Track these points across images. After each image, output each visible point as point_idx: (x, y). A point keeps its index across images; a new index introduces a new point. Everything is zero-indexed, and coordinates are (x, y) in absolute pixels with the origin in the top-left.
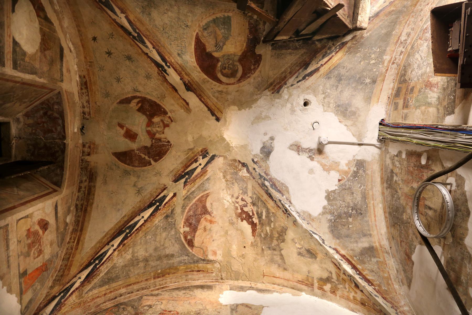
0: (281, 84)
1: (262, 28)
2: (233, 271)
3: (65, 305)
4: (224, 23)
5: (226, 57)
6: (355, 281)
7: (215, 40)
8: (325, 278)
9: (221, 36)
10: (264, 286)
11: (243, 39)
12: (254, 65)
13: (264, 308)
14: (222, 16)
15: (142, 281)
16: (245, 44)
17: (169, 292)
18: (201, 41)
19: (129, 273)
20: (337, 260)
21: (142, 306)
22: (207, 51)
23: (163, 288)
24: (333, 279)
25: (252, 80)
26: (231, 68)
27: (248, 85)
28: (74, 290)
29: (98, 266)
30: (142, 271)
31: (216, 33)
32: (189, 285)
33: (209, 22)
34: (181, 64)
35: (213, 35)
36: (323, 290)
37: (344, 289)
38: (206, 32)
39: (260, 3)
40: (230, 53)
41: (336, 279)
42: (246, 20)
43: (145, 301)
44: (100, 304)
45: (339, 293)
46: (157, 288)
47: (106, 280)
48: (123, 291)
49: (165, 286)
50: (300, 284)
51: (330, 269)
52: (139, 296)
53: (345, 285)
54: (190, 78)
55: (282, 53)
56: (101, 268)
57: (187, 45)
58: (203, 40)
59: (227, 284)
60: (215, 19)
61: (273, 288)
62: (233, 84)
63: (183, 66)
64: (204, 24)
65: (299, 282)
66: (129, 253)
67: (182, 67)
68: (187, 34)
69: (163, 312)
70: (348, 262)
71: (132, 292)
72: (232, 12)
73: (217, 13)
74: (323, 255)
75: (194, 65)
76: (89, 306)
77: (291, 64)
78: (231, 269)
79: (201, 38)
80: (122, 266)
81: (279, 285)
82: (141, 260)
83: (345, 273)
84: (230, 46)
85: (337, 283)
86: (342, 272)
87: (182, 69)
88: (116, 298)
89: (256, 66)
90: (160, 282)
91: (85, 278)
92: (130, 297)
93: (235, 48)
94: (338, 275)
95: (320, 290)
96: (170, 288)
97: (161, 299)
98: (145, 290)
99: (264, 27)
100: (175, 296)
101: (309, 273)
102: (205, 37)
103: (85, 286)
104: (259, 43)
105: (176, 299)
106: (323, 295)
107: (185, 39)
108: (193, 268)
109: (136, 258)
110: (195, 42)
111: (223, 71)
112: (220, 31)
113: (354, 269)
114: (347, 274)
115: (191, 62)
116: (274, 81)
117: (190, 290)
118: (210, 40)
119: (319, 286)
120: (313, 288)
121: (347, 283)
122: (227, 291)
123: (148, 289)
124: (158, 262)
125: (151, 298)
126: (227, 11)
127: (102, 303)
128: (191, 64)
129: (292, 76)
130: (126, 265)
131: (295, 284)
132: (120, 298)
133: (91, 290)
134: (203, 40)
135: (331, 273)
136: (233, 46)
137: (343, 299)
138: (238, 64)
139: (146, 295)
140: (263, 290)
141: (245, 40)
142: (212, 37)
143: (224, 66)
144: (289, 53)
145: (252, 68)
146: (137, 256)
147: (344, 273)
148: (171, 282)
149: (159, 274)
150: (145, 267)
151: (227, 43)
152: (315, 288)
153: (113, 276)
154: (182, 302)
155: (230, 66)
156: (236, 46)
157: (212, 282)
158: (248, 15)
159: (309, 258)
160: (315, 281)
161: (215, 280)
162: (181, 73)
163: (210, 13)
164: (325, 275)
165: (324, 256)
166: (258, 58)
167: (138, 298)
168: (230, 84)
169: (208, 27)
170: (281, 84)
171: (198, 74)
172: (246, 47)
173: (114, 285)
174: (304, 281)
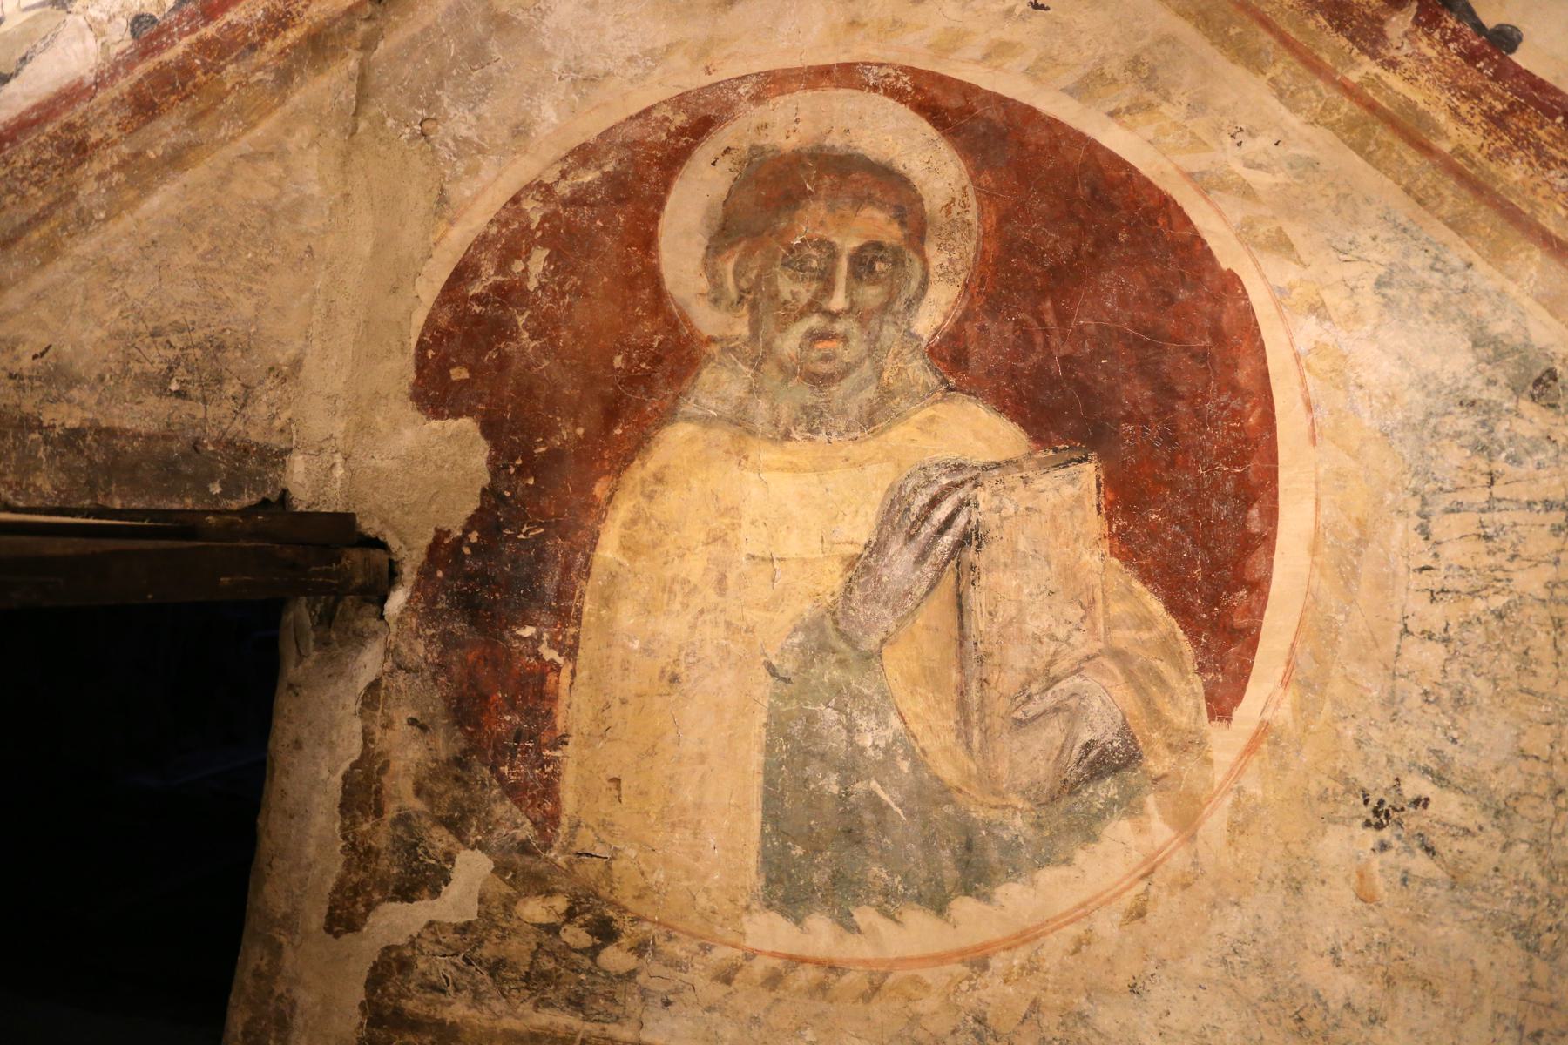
0: (209, 31)
1: (401, 725)
4: (851, 835)
5: (852, 395)
7: (979, 623)
9: (897, 665)
11: (626, 616)
12: (508, 294)
14: (865, 916)
16: (608, 550)
18: (1172, 608)
22: (1089, 472)
25: (548, 114)
26: (795, 262)
27: (600, 66)
31: (962, 706)
33: (1046, 862)
34: (1497, 255)
35: (1007, 683)
38: (1098, 728)
39: (415, 1025)
40: (800, 449)
42: (585, 840)
54: (1347, 89)
55: (163, 391)
57: (1401, 532)
58: (1147, 622)
60: (967, 890)
62: (775, 82)
63: (1458, 225)
64: (1119, 830)
67: (1484, 216)
68: (1391, 702)
72: (751, 955)
73: (941, 959)
75: (1284, 273)
77: (51, 251)
79: (1166, 647)
84: (792, 546)
87: (1478, 188)
89: (489, 275)
93: (731, 511)
99: (367, 736)
102: (1119, 655)
104: (442, 551)
107: (1436, 615)
110: (1259, 587)
111: (892, 234)
112: (906, 740)
115: (1333, 298)
116: (285, 78)
118: (1032, 626)
126: (807, 976)
128: (1336, 272)
129: (47, 109)
134: (1147, 622)
136: (751, 540)
138: (706, 320)
141: (607, 601)
142: (1018, 658)
143: (871, 295)
144: (74, 381)
145: (538, 261)
151: (833, 579)
155: (805, 291)
156: (716, 538)
158: (560, 903)
162: (1496, 121)
163: (1031, 968)
166: (459, 374)
168: (821, 76)
169: (1073, 791)
170: (209, 31)
171: (1229, 159)
172: (596, 510)
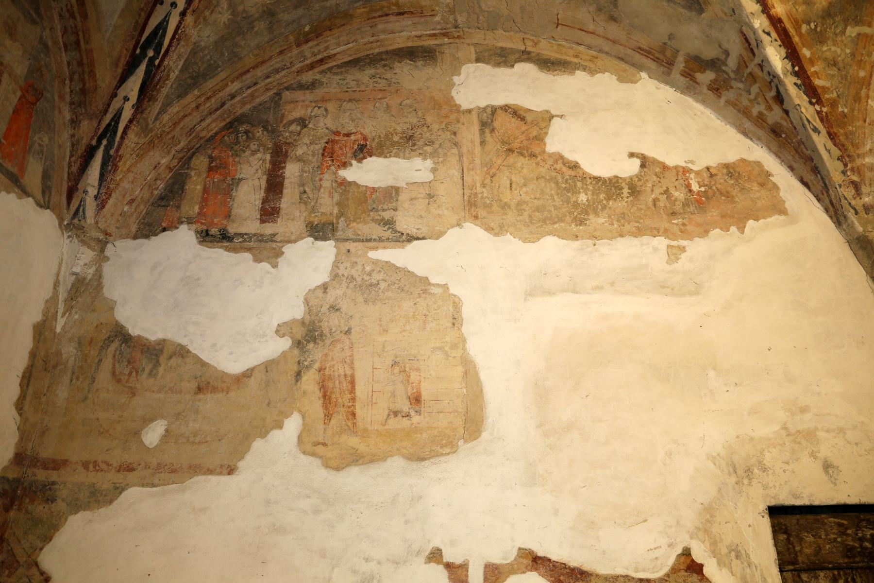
2: (483, 11)
3: (121, 157)
6: (781, 89)
8: (709, 59)
10: (555, 47)
13: (553, 121)
15: (270, 58)
17: (337, 74)
19: (236, 50)
20: (754, 32)
21: (285, 122)
23: (321, 61)
24: (726, 65)
28: (127, 125)
29: (157, 62)
30: (266, 39)
32: (382, 49)
36: (691, 80)
37: (744, 93)
41: (735, 69)
43: (288, 107)
44: (195, 126)
45: (730, 95)
46: (308, 62)
47: (189, 81)
48: (234, 87)
49: (325, 54)
50: (642, 54)
51: (726, 46)
52: (272, 92)
53: (751, 86)
56: (166, 63)
59: (468, 41)
61: (576, 56)
65: (639, 50)
66: (223, 8)
69: (333, 137)
70: (782, 40)
71: (255, 84)
74: (722, 11)
76: (173, 137)
78: (480, 7)
80: (215, 42)
81: (589, 47)
82: (257, 15)
83: (764, 64)
85: (732, 75)
86: (757, 60)
88: (223, 104)
90: (313, 50)
91: (139, 96)
92: (253, 96)
94: (743, 64)
95: (686, 77)
96: (339, 62)
97: (324, 100)
98: (284, 73)
100: (353, 84)
101: (670, 39)
103: (145, 109)
105: (356, 95)
106: (687, 88)
108: (385, 9)
109: (244, 15)
113: (790, 60)
114: (766, 69)
117: (385, 66)
119: (687, 70)
120: (671, 70)
121: (757, 85)
122: (470, 65)
123: (288, 68)
124: (300, 11)
125: (299, 95)
127: (198, 124)
130: (223, 36)
131: (630, 52)
132: (232, 102)
133: (163, 110)
135: (727, 53)
137: (733, 109)
139: (287, 89)
140: (553, 63)
146: (244, 10)
147: (759, 65)
148: (339, 45)
149: (307, 34)
150: (270, 29)
152: (674, 70)
153: (201, 69)
154: (370, 106)
157: (434, 35)
159: (683, 7)
160: (681, 59)
161: (441, 29)
164: (710, 53)
165: (726, 14)
167: (272, 99)
173: (210, 83)
174: (653, 51)
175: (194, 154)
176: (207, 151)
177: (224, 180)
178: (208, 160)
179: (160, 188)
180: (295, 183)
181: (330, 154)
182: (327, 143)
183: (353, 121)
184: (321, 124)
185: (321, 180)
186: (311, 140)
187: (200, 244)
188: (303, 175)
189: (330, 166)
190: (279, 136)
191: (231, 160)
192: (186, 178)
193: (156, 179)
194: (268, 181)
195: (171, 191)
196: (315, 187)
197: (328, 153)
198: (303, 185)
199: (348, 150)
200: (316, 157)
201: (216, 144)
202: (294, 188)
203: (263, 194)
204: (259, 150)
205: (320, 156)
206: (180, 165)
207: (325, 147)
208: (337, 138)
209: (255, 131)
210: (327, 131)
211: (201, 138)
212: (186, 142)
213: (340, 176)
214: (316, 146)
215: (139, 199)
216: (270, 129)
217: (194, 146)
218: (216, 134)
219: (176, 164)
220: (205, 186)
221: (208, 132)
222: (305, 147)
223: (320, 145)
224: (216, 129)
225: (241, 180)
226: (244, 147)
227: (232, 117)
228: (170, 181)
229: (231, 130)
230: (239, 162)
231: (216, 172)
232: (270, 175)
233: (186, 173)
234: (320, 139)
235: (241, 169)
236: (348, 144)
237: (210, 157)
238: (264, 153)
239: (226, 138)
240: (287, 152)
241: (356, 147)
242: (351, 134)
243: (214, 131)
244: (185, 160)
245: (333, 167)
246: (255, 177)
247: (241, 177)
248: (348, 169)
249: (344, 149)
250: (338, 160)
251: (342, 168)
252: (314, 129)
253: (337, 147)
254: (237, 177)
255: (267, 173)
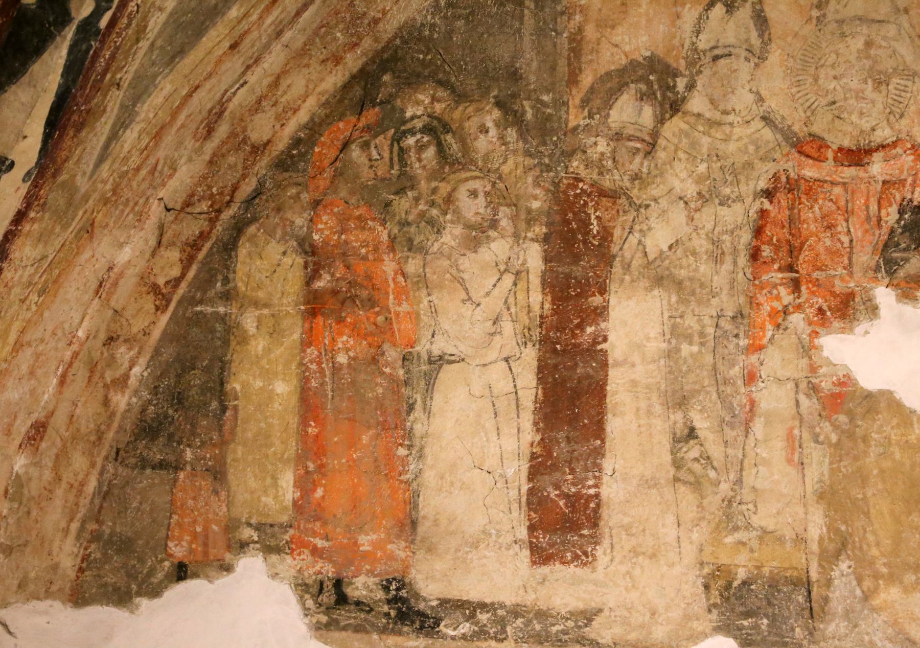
175: (238, 228)
176: (289, 215)
177: (374, 360)
178: (300, 261)
179: (133, 382)
180: (648, 387)
181: (783, 253)
182: (769, 194)
183: (881, 82)
184: (742, 99)
185: (751, 378)
186: (700, 180)
187: (320, 638)
188: (678, 350)
189: (786, 312)
190: (570, 154)
191: (389, 266)
192: (226, 343)
193: (111, 340)
194: (543, 371)
195: (179, 399)
196: (731, 408)
197: (777, 249)
198: (681, 401)
199: (857, 233)
200: (727, 266)
201: (323, 182)
202: (649, 413)
203: (529, 435)
204: (494, 224)
205: (743, 260)
206: (191, 274)
207: (763, 213)
208: (810, 172)
209: (472, 126)
210: (768, 134)
211: (258, 150)
212: (199, 166)
213: (830, 363)
214: (723, 211)
215: (60, 420)
216: (529, 115)
217: (235, 188)
218: (314, 129)
219: (176, 272)
220: (304, 381)
221: (281, 119)
222: (678, 215)
223: (738, 208)
224: (311, 102)
225: (439, 361)
226: (433, 204)
227: (367, 43)
228: (169, 353)
229: (371, 115)
230: (422, 281)
231: (340, 321)
232: (546, 344)
233: (223, 319)
234: (736, 173)
235: (434, 311)
236: (860, 202)
237: (308, 248)
238: (516, 236)
239: (355, 152)
240: (606, 235)
241: (891, 215)
242: (869, 152)
243: (303, 116)
244: (210, 254)
245: (796, 320)
246: (492, 355)
247: (436, 352)
248: (859, 329)
249: (841, 227)
250: (817, 283)
251: (837, 324)
252: (713, 124)
253: (810, 215)
254: (422, 348)
255: (536, 333)
